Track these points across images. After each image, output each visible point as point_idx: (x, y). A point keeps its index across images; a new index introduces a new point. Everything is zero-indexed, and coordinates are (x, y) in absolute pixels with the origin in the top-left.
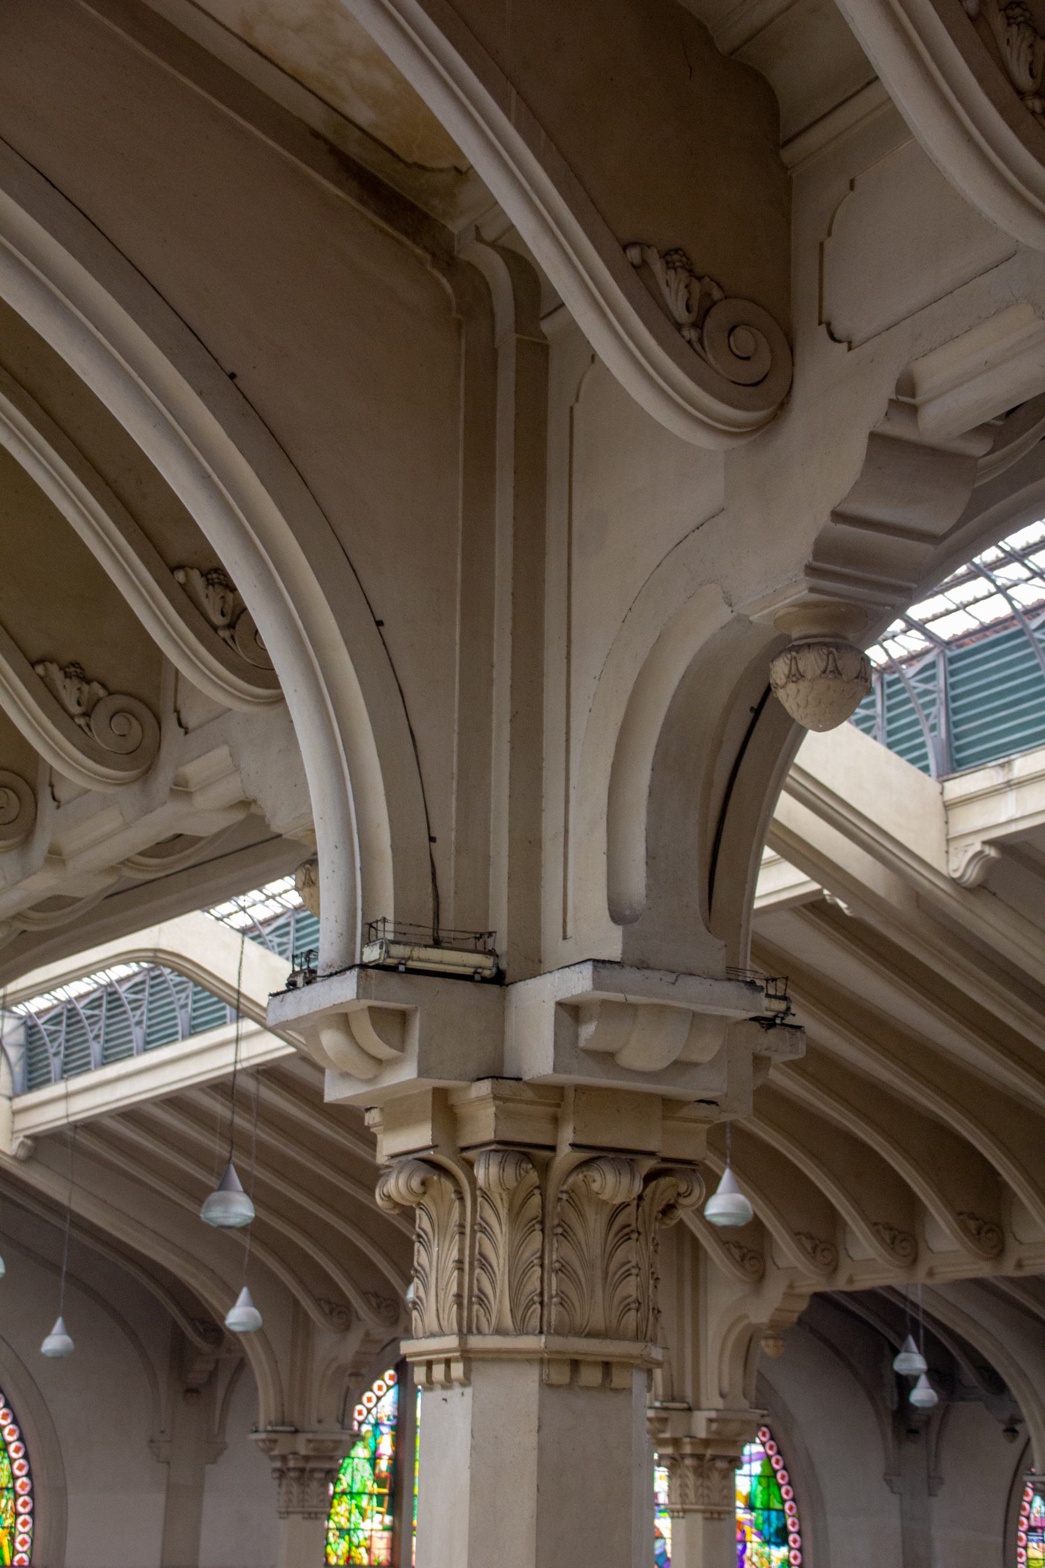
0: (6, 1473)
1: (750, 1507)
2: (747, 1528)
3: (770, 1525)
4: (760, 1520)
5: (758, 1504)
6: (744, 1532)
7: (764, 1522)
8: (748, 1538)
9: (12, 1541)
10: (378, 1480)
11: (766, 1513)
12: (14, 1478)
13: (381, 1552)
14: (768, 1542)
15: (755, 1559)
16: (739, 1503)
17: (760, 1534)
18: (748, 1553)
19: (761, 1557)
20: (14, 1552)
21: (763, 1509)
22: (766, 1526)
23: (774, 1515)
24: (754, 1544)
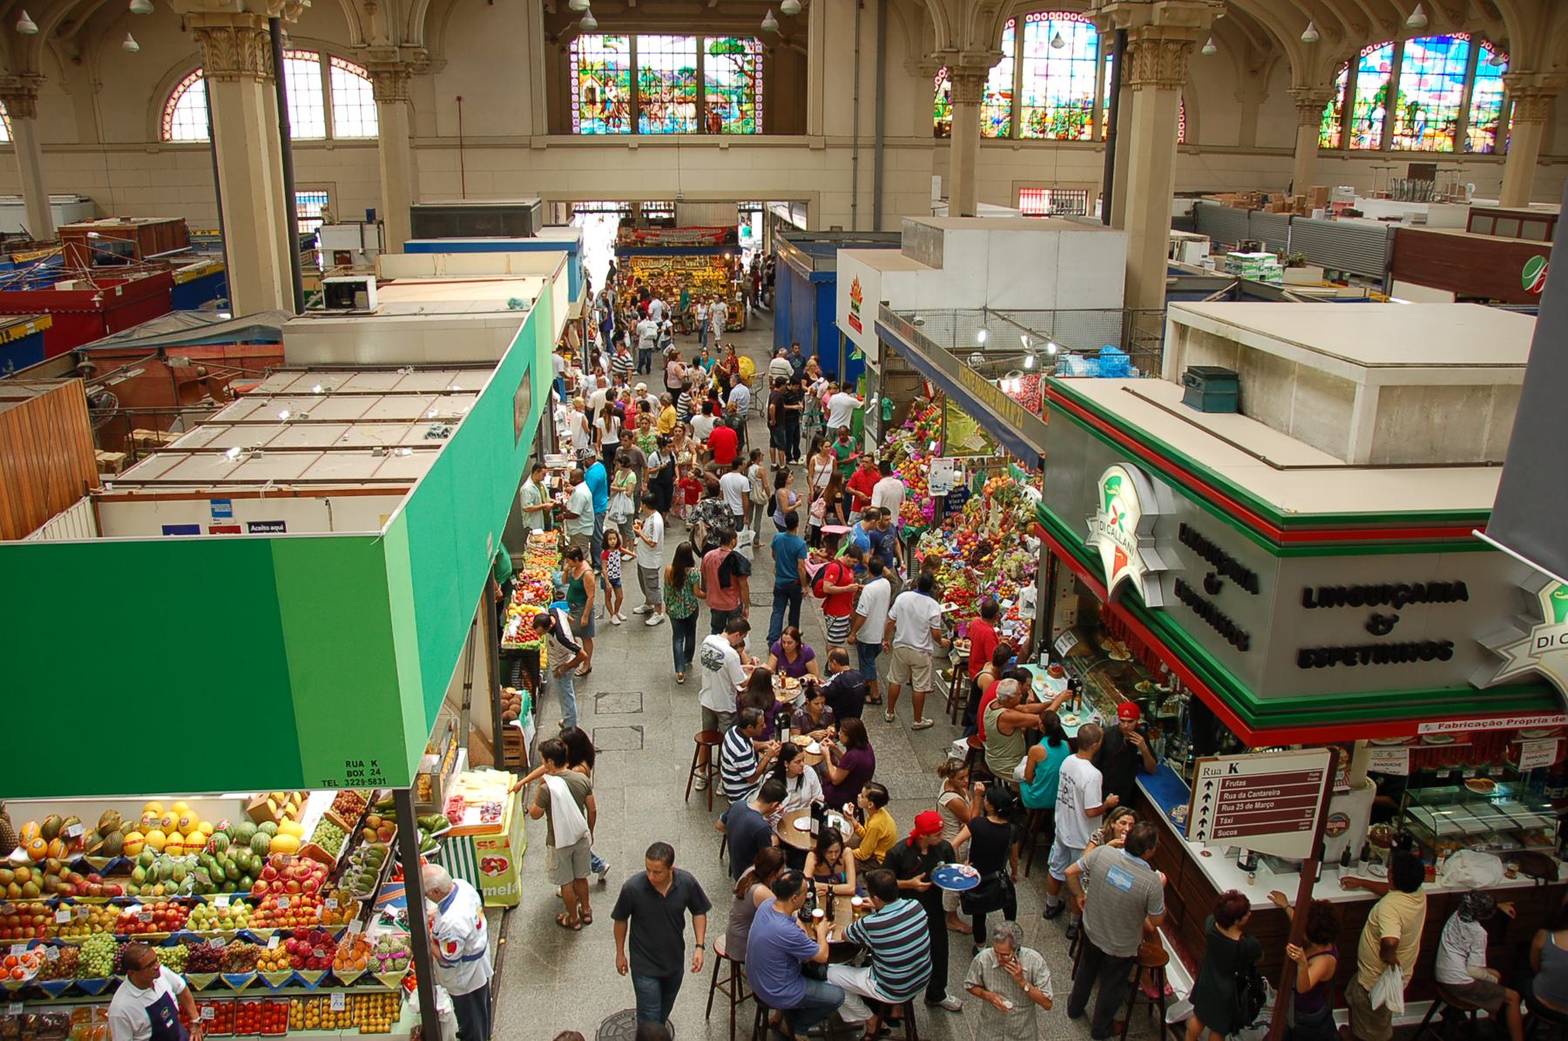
10: (1336, 111)
13: (1335, 143)
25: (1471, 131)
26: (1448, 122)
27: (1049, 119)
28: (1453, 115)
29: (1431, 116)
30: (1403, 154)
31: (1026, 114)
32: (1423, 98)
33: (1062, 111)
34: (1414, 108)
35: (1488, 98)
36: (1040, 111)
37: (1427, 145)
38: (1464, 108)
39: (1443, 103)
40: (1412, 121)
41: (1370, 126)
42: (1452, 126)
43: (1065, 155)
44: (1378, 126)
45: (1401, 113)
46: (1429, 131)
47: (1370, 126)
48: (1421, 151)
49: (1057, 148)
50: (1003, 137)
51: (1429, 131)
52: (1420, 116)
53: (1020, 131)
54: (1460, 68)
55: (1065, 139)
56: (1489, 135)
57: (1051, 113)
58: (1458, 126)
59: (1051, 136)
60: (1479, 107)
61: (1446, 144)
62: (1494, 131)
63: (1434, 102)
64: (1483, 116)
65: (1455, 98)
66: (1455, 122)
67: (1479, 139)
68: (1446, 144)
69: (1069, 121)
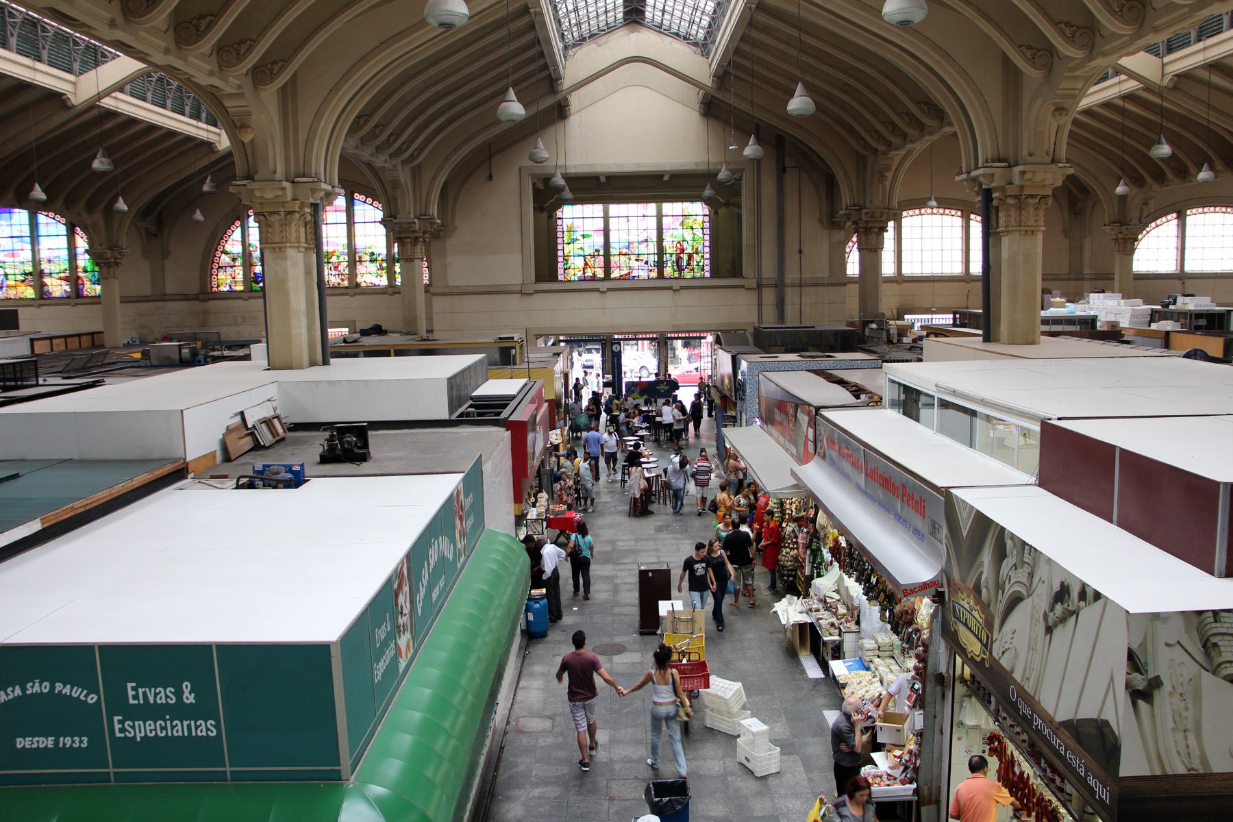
1: (85, 271)
25: (47, 280)
26: (26, 274)
28: (29, 269)
29: (8, 271)
35: (55, 253)
37: (12, 294)
39: (16, 259)
42: (29, 277)
46: (11, 282)
51: (11, 282)
54: (26, 230)
56: (63, 283)
58: (37, 276)
60: (50, 261)
61: (30, 293)
64: (54, 268)
65: (27, 255)
66: (30, 274)
67: (57, 288)
68: (30, 293)
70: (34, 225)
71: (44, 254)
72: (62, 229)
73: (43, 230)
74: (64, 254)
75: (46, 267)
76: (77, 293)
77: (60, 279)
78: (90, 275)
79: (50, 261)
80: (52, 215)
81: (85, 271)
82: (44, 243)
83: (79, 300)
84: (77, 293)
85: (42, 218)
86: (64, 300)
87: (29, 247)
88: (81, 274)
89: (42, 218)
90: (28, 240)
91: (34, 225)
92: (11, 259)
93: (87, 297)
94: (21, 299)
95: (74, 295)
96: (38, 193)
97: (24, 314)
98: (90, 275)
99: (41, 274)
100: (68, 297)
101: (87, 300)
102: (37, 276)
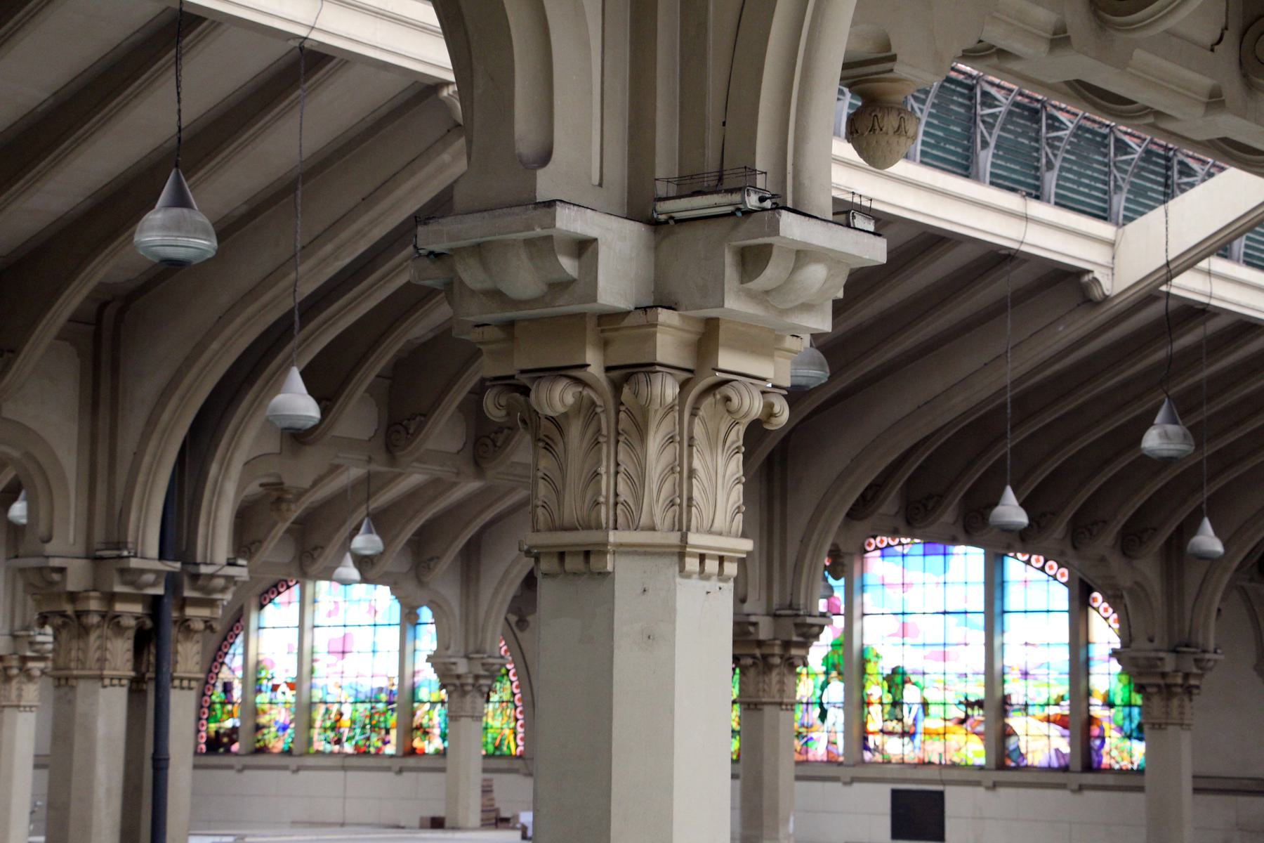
0: (509, 692)
1: (1109, 704)
2: (1106, 725)
3: (1131, 721)
4: (1120, 716)
5: (1118, 701)
6: (1102, 730)
7: (1124, 718)
8: (1107, 734)
9: (515, 738)
11: (1127, 709)
12: (514, 695)
14: (1129, 737)
15: (1114, 753)
16: (1096, 700)
17: (1121, 729)
18: (1106, 748)
19: (1121, 752)
20: (517, 746)
21: (1124, 706)
22: (1127, 722)
23: (1136, 711)
24: (1113, 739)
25: (1015, 721)
26: (969, 704)
27: (346, 721)
28: (977, 691)
30: (885, 770)
31: (318, 715)
32: (911, 661)
33: (361, 707)
34: (897, 680)
36: (335, 708)
37: (934, 751)
38: (994, 676)
40: (897, 704)
41: (823, 715)
42: (977, 713)
43: (357, 779)
44: (836, 717)
45: (876, 690)
47: (823, 715)
48: (924, 764)
49: (344, 768)
50: (288, 752)
51: (933, 722)
52: (911, 695)
53: (310, 742)
55: (367, 754)
56: (1055, 730)
57: (347, 710)
59: (348, 748)
61: (973, 751)
62: (1062, 722)
63: (934, 667)
66: (980, 704)
67: (1041, 742)
68: (973, 751)
69: (373, 725)
70: (994, 585)
71: (1013, 657)
72: (1060, 596)
73: (1014, 597)
74: (1062, 658)
75: (1015, 689)
76: (1086, 758)
77: (1048, 719)
78: (1118, 714)
79: (1025, 674)
80: (1038, 560)
81: (1109, 704)
82: (1015, 629)
83: (1089, 778)
84: (1086, 758)
85: (1014, 567)
86: (1052, 776)
87: (980, 636)
88: (1097, 711)
89: (1014, 567)
90: (980, 619)
91: (994, 585)
92: (940, 666)
93: (1110, 770)
94: (954, 765)
95: (1077, 765)
96: (1011, 511)
97: (957, 803)
98: (1118, 714)
99: (1004, 705)
100: (1065, 769)
101: (1110, 780)
102: (994, 709)
